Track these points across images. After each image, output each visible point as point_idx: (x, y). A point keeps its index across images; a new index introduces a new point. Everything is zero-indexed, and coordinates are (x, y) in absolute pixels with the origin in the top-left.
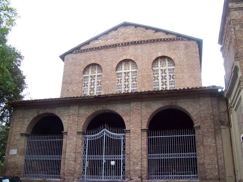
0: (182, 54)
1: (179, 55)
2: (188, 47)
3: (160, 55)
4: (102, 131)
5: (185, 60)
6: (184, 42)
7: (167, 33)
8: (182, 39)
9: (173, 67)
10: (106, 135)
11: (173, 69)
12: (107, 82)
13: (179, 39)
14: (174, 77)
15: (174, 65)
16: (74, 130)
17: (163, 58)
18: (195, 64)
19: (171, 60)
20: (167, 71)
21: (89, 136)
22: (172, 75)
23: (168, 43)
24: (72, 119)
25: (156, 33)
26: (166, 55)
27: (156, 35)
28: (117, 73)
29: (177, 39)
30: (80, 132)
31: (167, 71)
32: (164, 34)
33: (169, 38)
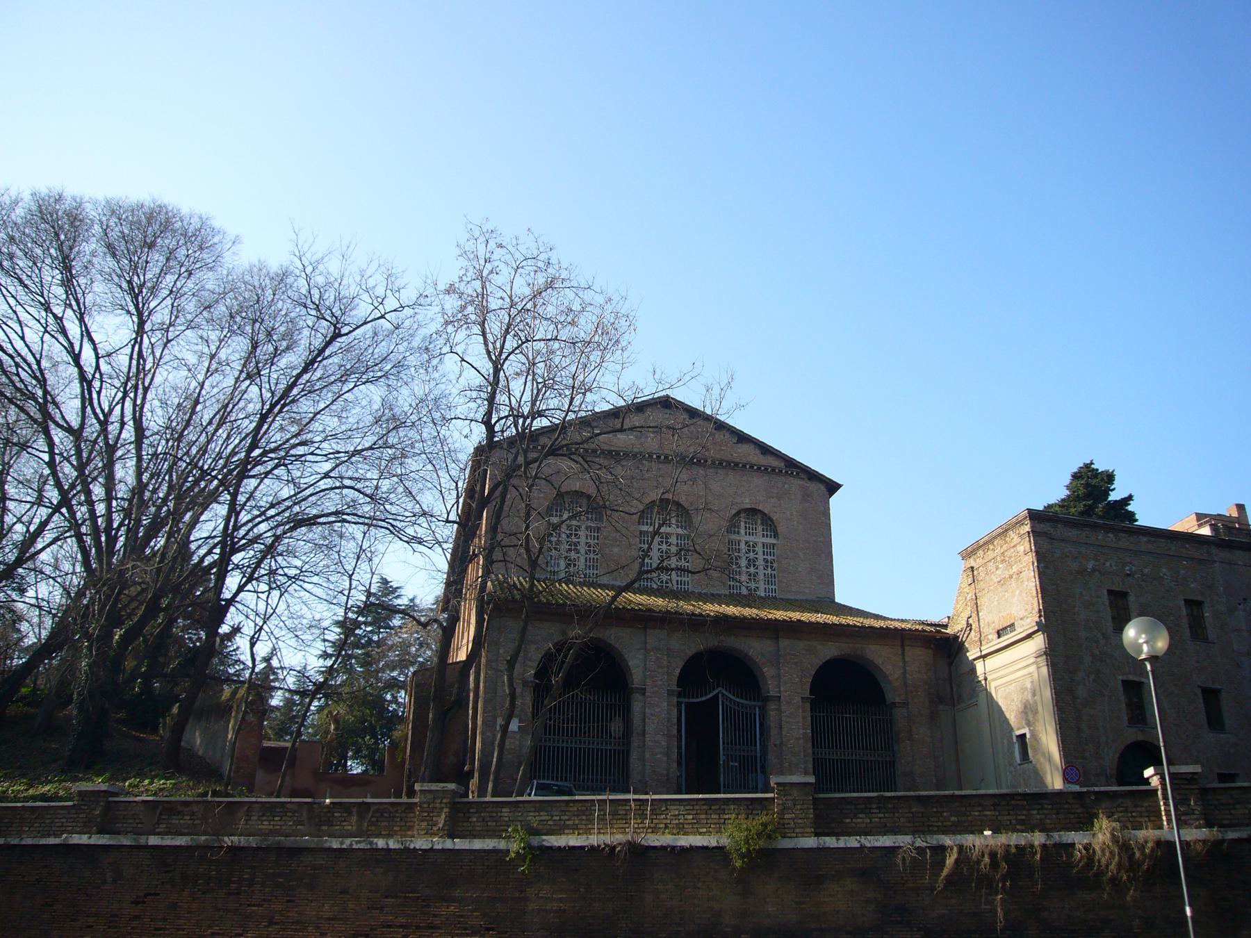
0: (794, 513)
1: (788, 513)
2: (808, 496)
3: (747, 503)
4: (716, 692)
5: (801, 527)
6: (801, 482)
7: (765, 449)
8: (798, 473)
9: (773, 541)
10: (723, 702)
11: (774, 545)
12: (616, 550)
13: (792, 473)
14: (775, 565)
15: (776, 536)
16: (661, 685)
17: (752, 512)
18: (820, 541)
19: (769, 522)
20: (759, 549)
21: (686, 700)
22: (769, 558)
23: (766, 477)
24: (653, 659)
25: (739, 445)
26: (760, 508)
27: (739, 451)
28: (641, 532)
29: (786, 472)
30: (673, 691)
31: (759, 549)
32: (758, 452)
33: (770, 467)
